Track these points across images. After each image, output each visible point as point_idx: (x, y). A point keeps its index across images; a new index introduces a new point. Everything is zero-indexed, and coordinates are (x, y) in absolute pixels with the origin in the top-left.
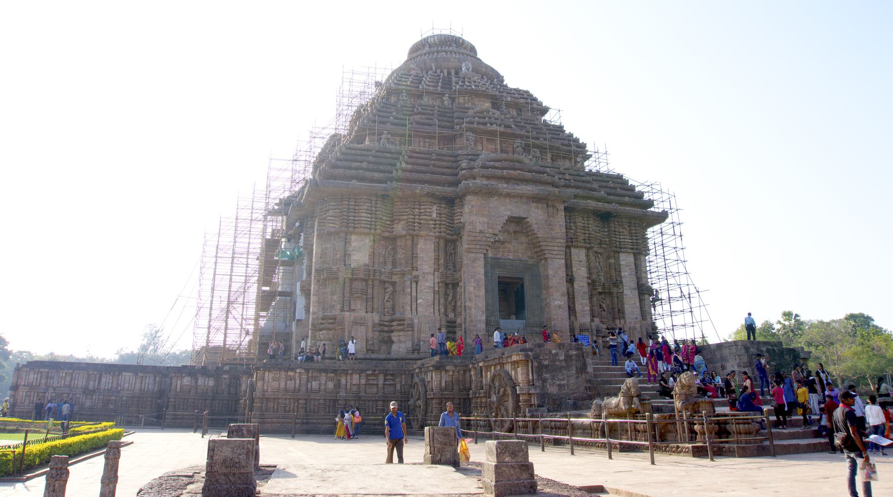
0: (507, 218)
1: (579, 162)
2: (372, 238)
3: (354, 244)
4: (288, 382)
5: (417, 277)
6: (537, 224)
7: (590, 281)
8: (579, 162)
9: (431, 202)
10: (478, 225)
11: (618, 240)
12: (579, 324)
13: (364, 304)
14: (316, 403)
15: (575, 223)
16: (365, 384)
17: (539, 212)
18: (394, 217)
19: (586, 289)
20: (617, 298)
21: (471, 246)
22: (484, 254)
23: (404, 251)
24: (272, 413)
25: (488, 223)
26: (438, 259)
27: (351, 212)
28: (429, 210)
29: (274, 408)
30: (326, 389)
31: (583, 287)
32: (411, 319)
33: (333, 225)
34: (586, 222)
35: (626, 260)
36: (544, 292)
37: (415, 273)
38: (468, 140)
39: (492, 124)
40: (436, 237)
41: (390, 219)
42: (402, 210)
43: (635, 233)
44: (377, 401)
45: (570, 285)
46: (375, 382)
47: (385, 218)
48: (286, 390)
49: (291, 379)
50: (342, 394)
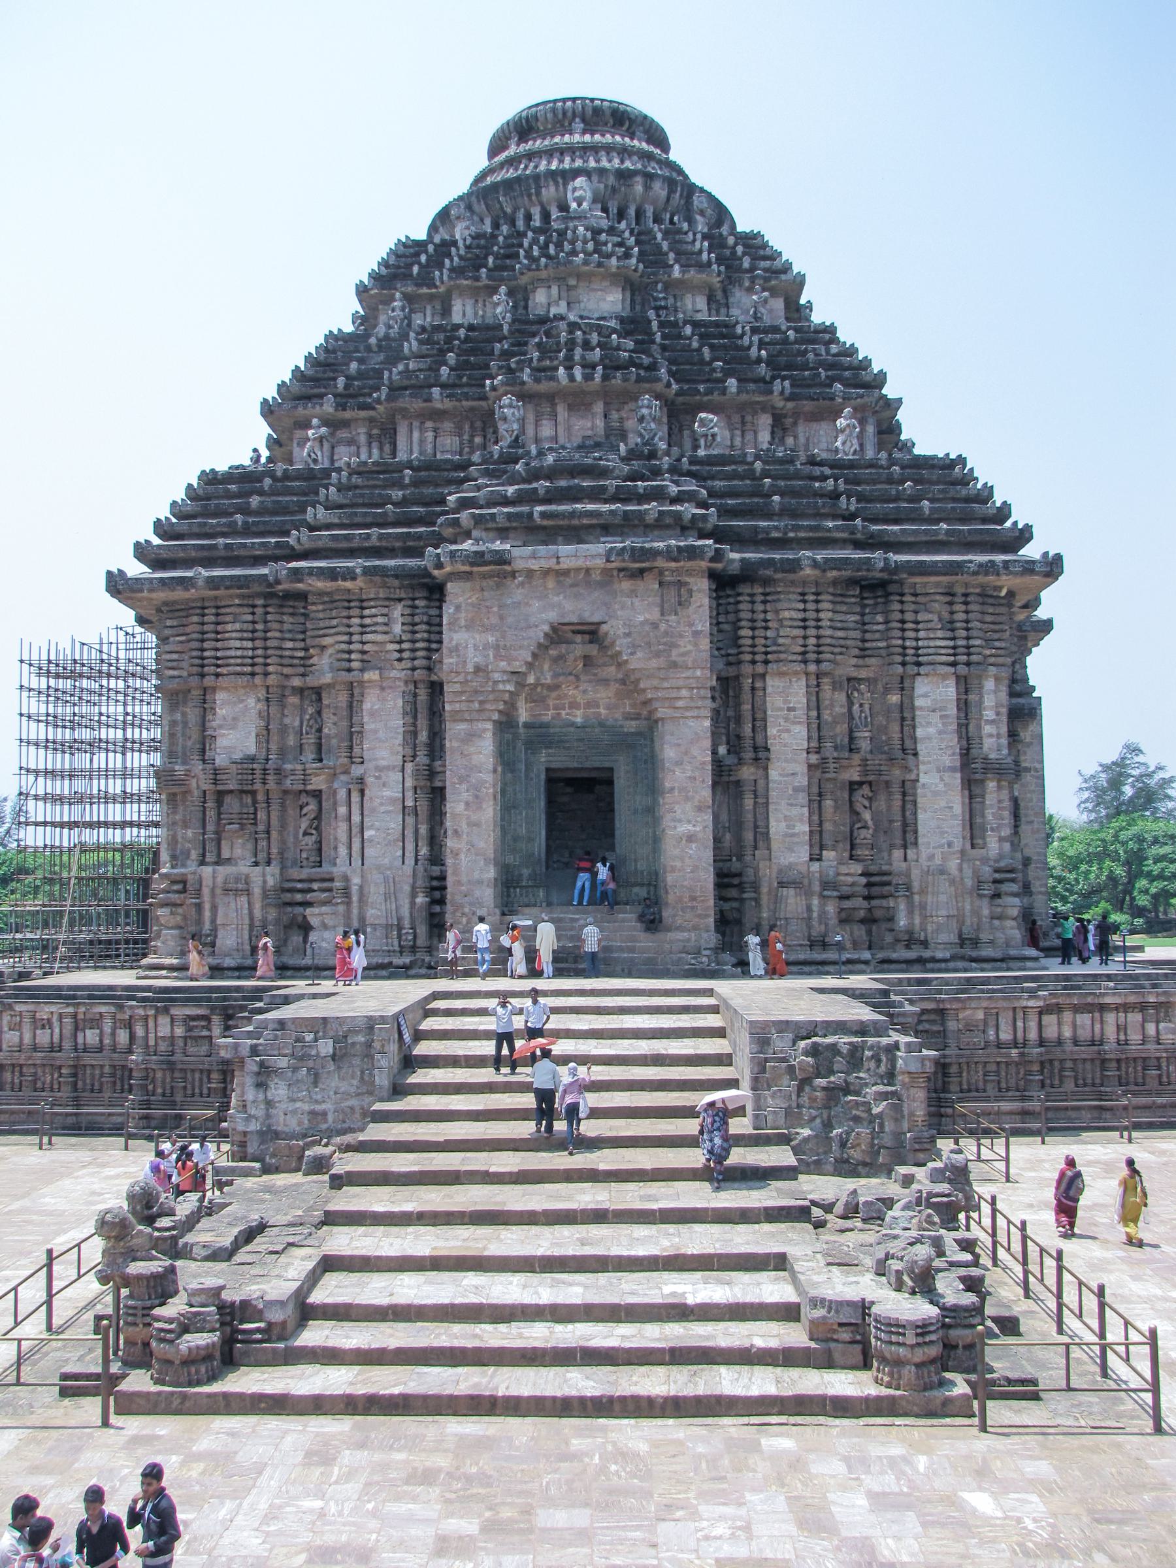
0: (546, 628)
1: (842, 431)
2: (262, 694)
3: (221, 712)
4: (38, 1032)
6: (628, 635)
7: (814, 759)
10: (471, 652)
11: (908, 643)
12: (775, 869)
13: (250, 846)
15: (777, 612)
16: (185, 1038)
18: (308, 641)
19: (802, 780)
20: (904, 794)
23: (335, 718)
24: (9, 1093)
26: (415, 734)
28: (380, 619)
29: (13, 1083)
32: (346, 879)
33: (175, 673)
37: (357, 771)
38: (505, 419)
41: (302, 645)
42: (322, 624)
44: (209, 1072)
45: (761, 772)
46: (205, 1033)
47: (290, 645)
48: (35, 1048)
49: (43, 1027)
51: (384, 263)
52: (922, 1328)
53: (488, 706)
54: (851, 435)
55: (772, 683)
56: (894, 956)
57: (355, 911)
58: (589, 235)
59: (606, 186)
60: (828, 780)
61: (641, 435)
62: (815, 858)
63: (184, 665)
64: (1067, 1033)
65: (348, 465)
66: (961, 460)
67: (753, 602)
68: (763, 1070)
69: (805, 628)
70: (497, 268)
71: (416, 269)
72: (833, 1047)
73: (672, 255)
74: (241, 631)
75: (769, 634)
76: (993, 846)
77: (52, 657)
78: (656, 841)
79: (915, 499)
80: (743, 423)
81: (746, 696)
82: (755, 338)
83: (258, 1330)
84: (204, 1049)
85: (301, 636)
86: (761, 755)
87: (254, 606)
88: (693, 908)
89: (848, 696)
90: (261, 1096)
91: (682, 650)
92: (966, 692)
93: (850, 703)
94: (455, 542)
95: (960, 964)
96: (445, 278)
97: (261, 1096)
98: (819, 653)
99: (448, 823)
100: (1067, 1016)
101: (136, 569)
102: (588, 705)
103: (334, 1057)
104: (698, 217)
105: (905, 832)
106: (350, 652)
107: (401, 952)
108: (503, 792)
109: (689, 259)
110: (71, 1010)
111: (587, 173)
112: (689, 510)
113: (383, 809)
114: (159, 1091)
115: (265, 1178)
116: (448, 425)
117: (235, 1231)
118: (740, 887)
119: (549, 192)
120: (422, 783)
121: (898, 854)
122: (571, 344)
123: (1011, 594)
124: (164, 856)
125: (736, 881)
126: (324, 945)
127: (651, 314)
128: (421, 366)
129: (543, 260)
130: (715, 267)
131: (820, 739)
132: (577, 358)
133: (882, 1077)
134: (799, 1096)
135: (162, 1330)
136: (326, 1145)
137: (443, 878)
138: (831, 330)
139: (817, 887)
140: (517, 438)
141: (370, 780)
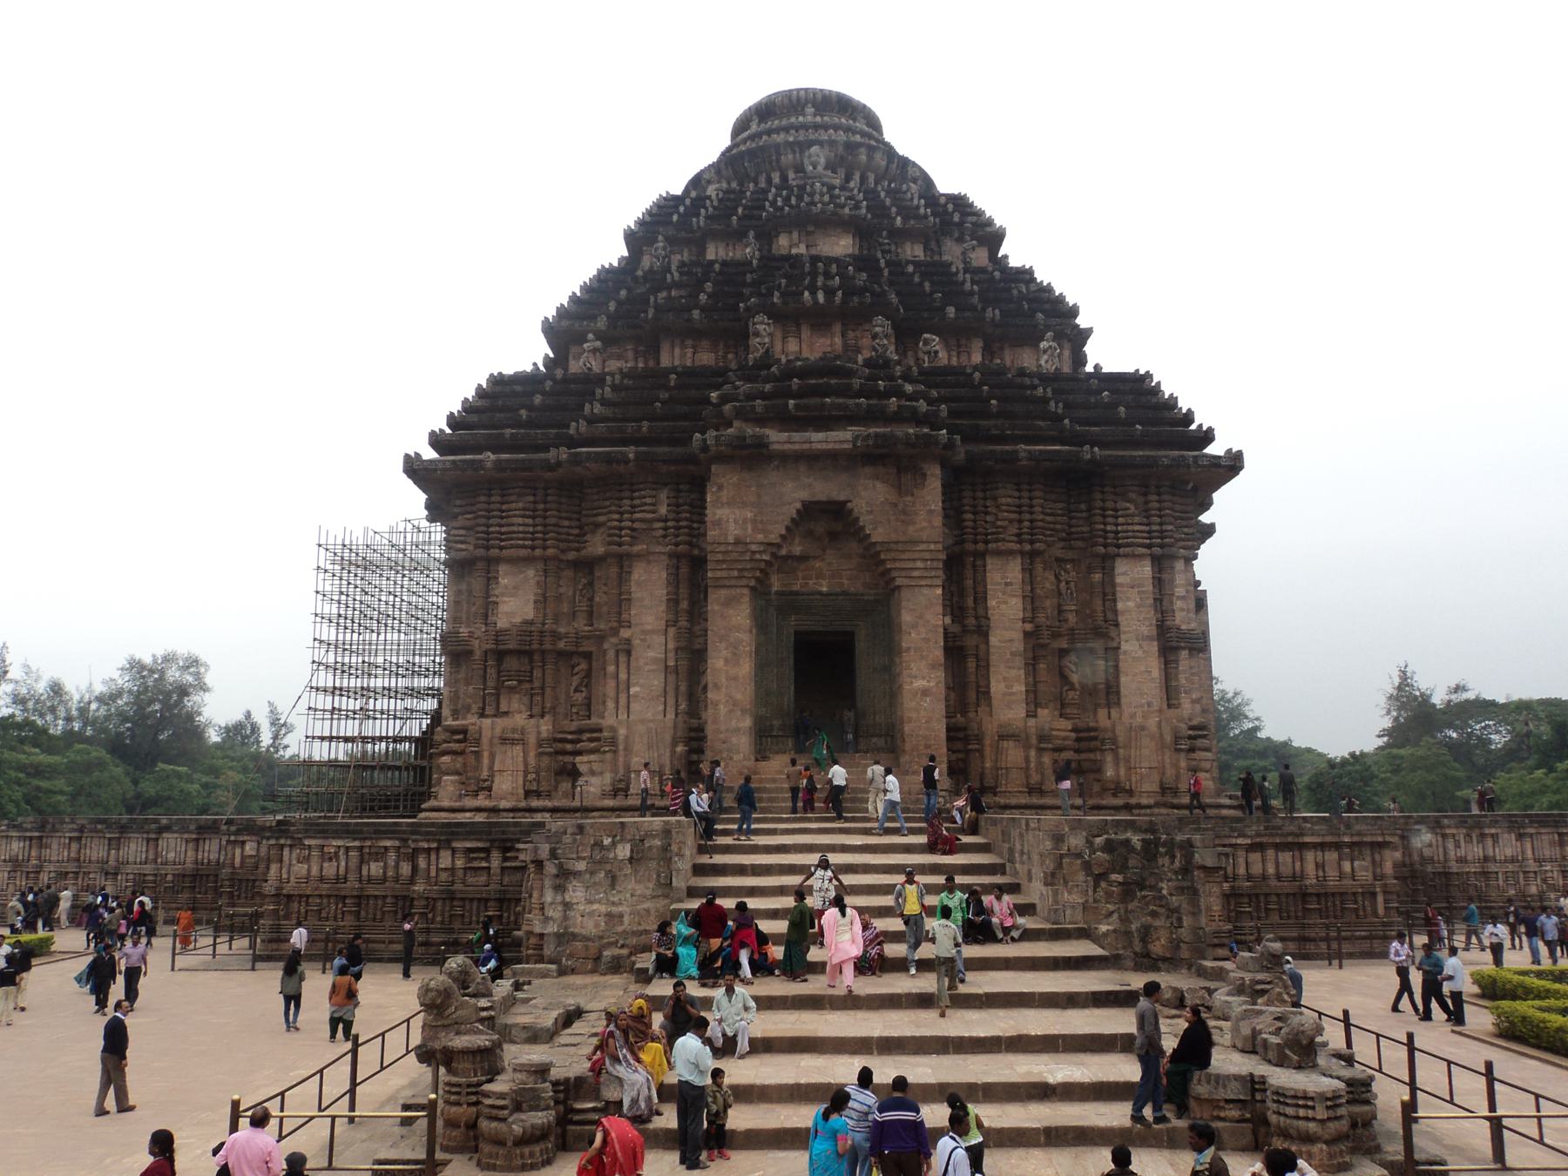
0: (798, 505)
1: (1045, 351)
2: (540, 566)
3: (504, 581)
5: (628, 641)
6: (871, 512)
8: (1045, 351)
9: (655, 483)
10: (732, 526)
11: (1109, 528)
13: (526, 700)
14: (380, 902)
15: (995, 498)
16: (465, 869)
17: (879, 485)
18: (584, 520)
19: (1019, 646)
22: (753, 589)
23: (605, 589)
25: (754, 521)
27: (494, 517)
28: (648, 500)
29: (299, 912)
30: (397, 879)
31: (1011, 641)
32: (613, 729)
33: (463, 546)
34: (1026, 494)
35: (1133, 575)
36: (897, 660)
37: (625, 633)
38: (757, 334)
39: (813, 293)
40: (671, 555)
41: (577, 523)
42: (596, 504)
43: (1160, 510)
44: (487, 900)
46: (484, 864)
47: (566, 523)
48: (321, 879)
49: (330, 859)
50: (419, 887)
51: (649, 212)
52: (1331, 1100)
53: (746, 574)
54: (1052, 355)
55: (992, 563)
56: (1104, 802)
57: (621, 759)
58: (825, 189)
59: (836, 156)
60: (1044, 646)
61: (874, 349)
62: (1031, 714)
63: (469, 539)
64: (1271, 870)
65: (621, 369)
66: (1148, 375)
67: (974, 491)
68: (1060, 866)
69: (1020, 513)
71: (675, 218)
72: (1128, 841)
73: (894, 210)
74: (524, 509)
75: (989, 518)
76: (1187, 707)
77: (347, 542)
78: (893, 695)
79: (1113, 406)
80: (959, 346)
81: (969, 572)
82: (968, 276)
83: (594, 1110)
84: (483, 879)
85: (575, 516)
86: (983, 621)
87: (536, 489)
89: (1056, 576)
90: (559, 898)
91: (918, 526)
92: (1160, 572)
93: (1059, 581)
94: (717, 430)
95: (1164, 811)
96: (702, 223)
97: (559, 898)
98: (1032, 535)
99: (709, 678)
100: (1270, 853)
101: (429, 454)
103: (631, 859)
105: (1108, 694)
106: (621, 529)
107: (662, 796)
108: (757, 652)
109: (908, 212)
110: (357, 843)
111: (821, 143)
112: (922, 405)
113: (647, 668)
114: (439, 919)
115: (560, 979)
116: (705, 343)
117: (555, 1014)
118: (966, 740)
119: (788, 158)
120: (683, 644)
121: (1102, 713)
122: (814, 274)
123: (1195, 489)
124: (446, 712)
125: (961, 735)
126: (592, 789)
127: (879, 255)
128: (683, 293)
129: (787, 208)
130: (932, 219)
131: (1033, 610)
132: (819, 284)
133: (1176, 873)
134: (1095, 891)
135: (493, 1107)
136: (623, 946)
137: (701, 729)
138: (1030, 272)
139: (1034, 741)
140: (767, 351)
141: (636, 642)
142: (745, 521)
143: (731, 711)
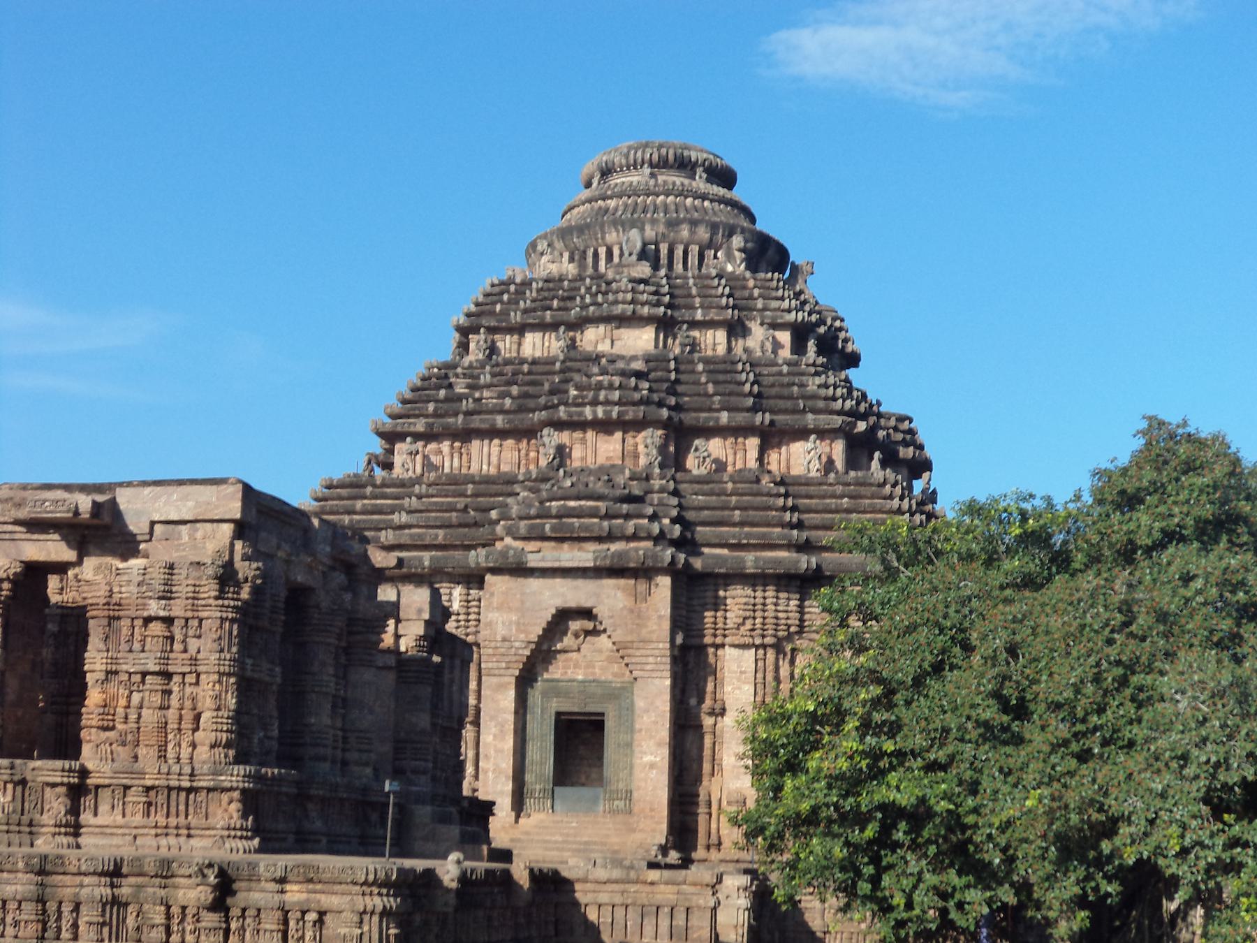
0: (554, 611)
6: (612, 617)
10: (500, 625)
17: (619, 594)
21: (490, 665)
25: (518, 624)
69: (754, 611)
70: (559, 309)
71: (498, 307)
73: (697, 300)
88: (652, 817)
91: (649, 629)
96: (518, 319)
98: (764, 630)
102: (587, 667)
104: (737, 254)
116: (510, 442)
119: (611, 237)
132: (602, 398)
142: (510, 623)
143: (496, 777)
